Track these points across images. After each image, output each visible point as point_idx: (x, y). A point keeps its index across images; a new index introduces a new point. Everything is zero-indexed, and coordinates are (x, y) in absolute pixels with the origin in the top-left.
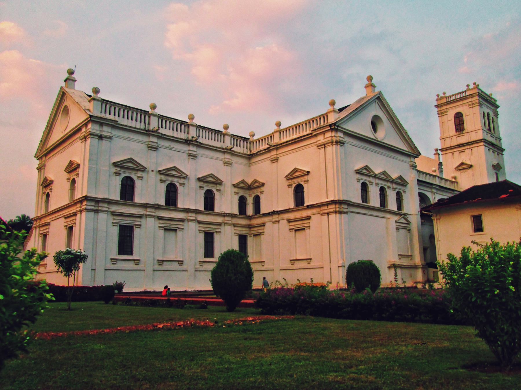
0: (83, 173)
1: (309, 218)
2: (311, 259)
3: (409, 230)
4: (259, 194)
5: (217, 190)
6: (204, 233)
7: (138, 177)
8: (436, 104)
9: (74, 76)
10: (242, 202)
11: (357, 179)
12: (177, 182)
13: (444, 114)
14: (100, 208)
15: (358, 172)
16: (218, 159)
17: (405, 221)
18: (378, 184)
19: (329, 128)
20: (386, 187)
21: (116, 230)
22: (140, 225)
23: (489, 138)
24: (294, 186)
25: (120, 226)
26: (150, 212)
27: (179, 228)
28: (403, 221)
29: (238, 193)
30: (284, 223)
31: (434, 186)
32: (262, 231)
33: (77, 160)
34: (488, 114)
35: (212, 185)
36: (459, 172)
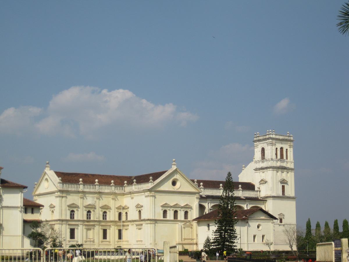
0: (57, 210)
1: (142, 225)
2: (142, 241)
3: (192, 228)
5: (108, 211)
10: (120, 214)
13: (257, 147)
15: (162, 206)
16: (109, 197)
23: (279, 164)
28: (188, 224)
29: (118, 211)
30: (135, 225)
33: (54, 204)
34: (282, 149)
36: (261, 185)
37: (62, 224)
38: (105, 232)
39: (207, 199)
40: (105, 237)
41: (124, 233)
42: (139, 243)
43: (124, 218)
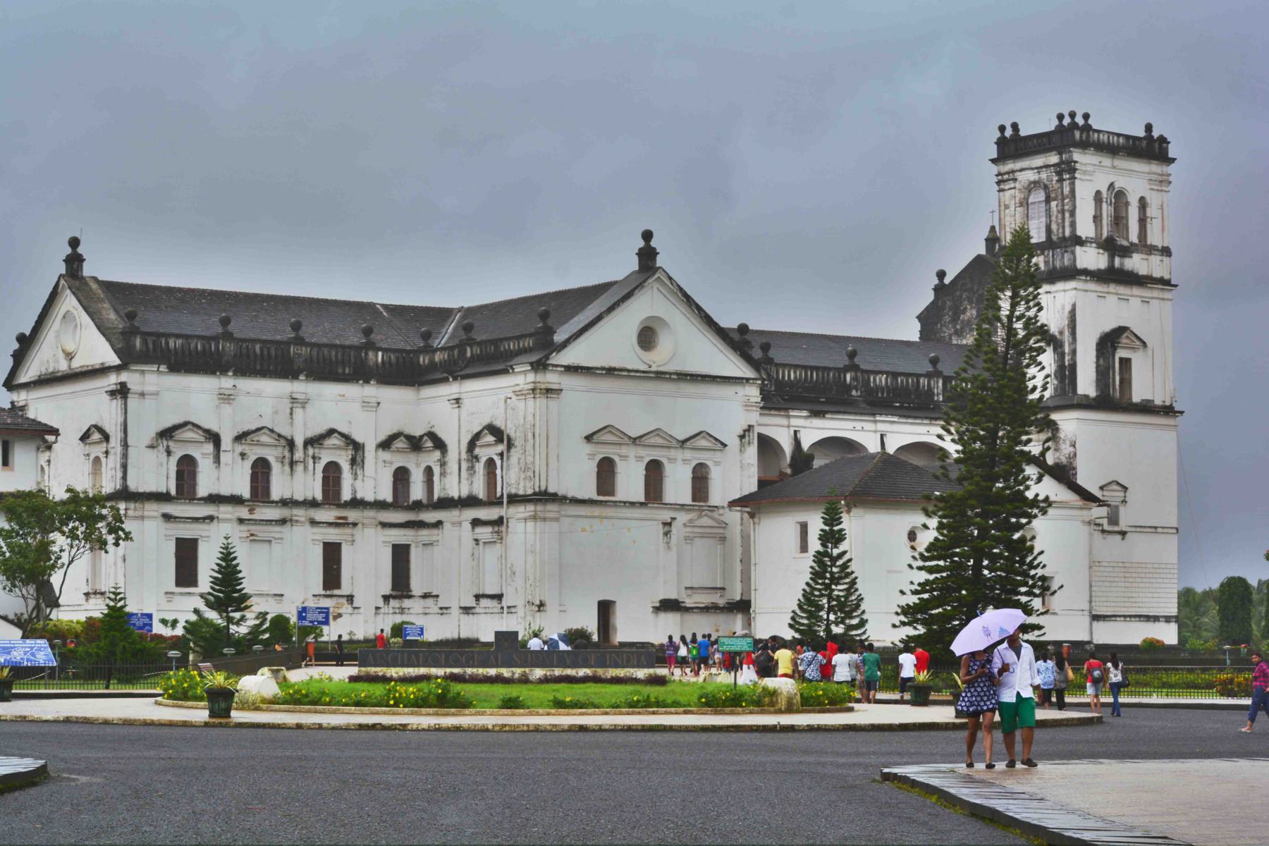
3: (723, 539)
4: (432, 464)
6: (322, 544)
7: (203, 454)
8: (995, 156)
9: (80, 250)
10: (401, 477)
11: (589, 454)
12: (271, 455)
14: (146, 513)
17: (709, 522)
18: (642, 457)
19: (530, 368)
20: (664, 461)
21: (171, 547)
22: (208, 537)
24: (483, 460)
25: (177, 539)
26: (225, 511)
27: (275, 539)
28: (705, 521)
30: (467, 526)
31: (878, 418)
32: (434, 538)
34: (1119, 197)
35: (338, 452)
37: (143, 518)
38: (332, 554)
39: (792, 413)
40: (332, 577)
41: (415, 556)
42: (484, 602)
43: (417, 491)
